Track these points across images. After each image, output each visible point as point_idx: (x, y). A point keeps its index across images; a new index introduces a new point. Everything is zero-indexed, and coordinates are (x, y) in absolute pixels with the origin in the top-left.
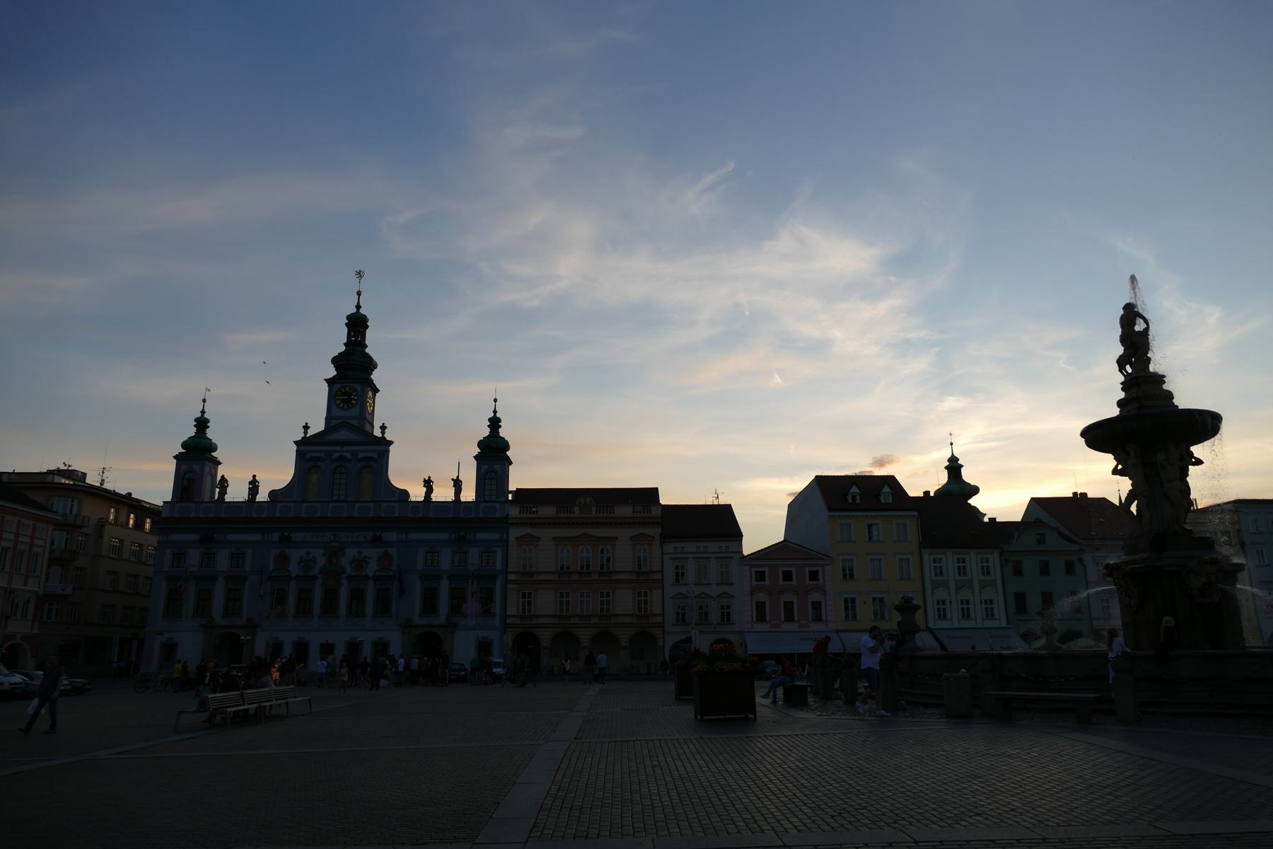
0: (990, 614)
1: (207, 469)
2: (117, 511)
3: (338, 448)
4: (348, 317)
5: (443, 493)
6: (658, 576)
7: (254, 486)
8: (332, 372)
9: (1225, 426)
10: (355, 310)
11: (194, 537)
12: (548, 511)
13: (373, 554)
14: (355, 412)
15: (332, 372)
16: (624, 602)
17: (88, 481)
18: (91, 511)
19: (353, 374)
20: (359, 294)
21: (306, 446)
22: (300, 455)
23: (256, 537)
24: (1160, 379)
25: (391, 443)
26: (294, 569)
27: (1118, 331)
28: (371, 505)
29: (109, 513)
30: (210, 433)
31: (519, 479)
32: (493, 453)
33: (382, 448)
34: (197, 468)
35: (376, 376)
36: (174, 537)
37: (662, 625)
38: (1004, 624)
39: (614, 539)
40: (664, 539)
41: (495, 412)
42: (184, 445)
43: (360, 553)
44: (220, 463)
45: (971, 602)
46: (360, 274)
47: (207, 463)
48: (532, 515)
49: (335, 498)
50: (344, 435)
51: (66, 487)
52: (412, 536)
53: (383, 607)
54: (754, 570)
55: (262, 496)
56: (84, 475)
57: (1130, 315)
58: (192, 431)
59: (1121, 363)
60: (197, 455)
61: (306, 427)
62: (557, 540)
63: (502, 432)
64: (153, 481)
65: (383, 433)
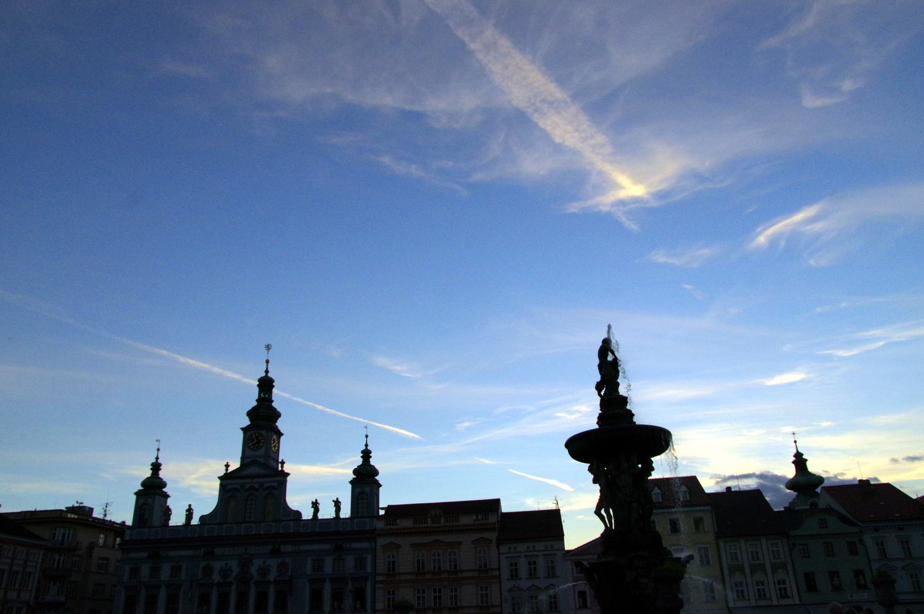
0: (784, 594)
2: (106, 536)
4: (260, 380)
5: (327, 512)
6: (496, 573)
7: (190, 513)
8: (246, 422)
9: (678, 436)
10: (264, 374)
11: (145, 555)
12: (407, 523)
13: (273, 563)
14: (262, 452)
15: (246, 422)
16: (469, 595)
17: (95, 515)
18: (84, 537)
19: (263, 424)
20: (267, 362)
21: (227, 479)
22: (222, 487)
24: (624, 400)
25: (288, 474)
26: (216, 577)
27: (597, 361)
29: (98, 538)
30: (162, 474)
31: (387, 498)
32: (365, 479)
34: (150, 501)
35: (280, 424)
36: (133, 555)
38: (797, 601)
39: (460, 543)
40: (499, 542)
41: (366, 445)
42: (143, 484)
44: (169, 496)
45: (766, 582)
46: (268, 347)
47: (157, 497)
48: (394, 527)
49: (247, 519)
50: (254, 470)
51: (80, 517)
55: (195, 521)
56: (91, 510)
57: (606, 348)
59: (599, 387)
60: (153, 491)
61: (227, 466)
62: (413, 545)
63: (373, 462)
64: (123, 513)
65: (282, 467)
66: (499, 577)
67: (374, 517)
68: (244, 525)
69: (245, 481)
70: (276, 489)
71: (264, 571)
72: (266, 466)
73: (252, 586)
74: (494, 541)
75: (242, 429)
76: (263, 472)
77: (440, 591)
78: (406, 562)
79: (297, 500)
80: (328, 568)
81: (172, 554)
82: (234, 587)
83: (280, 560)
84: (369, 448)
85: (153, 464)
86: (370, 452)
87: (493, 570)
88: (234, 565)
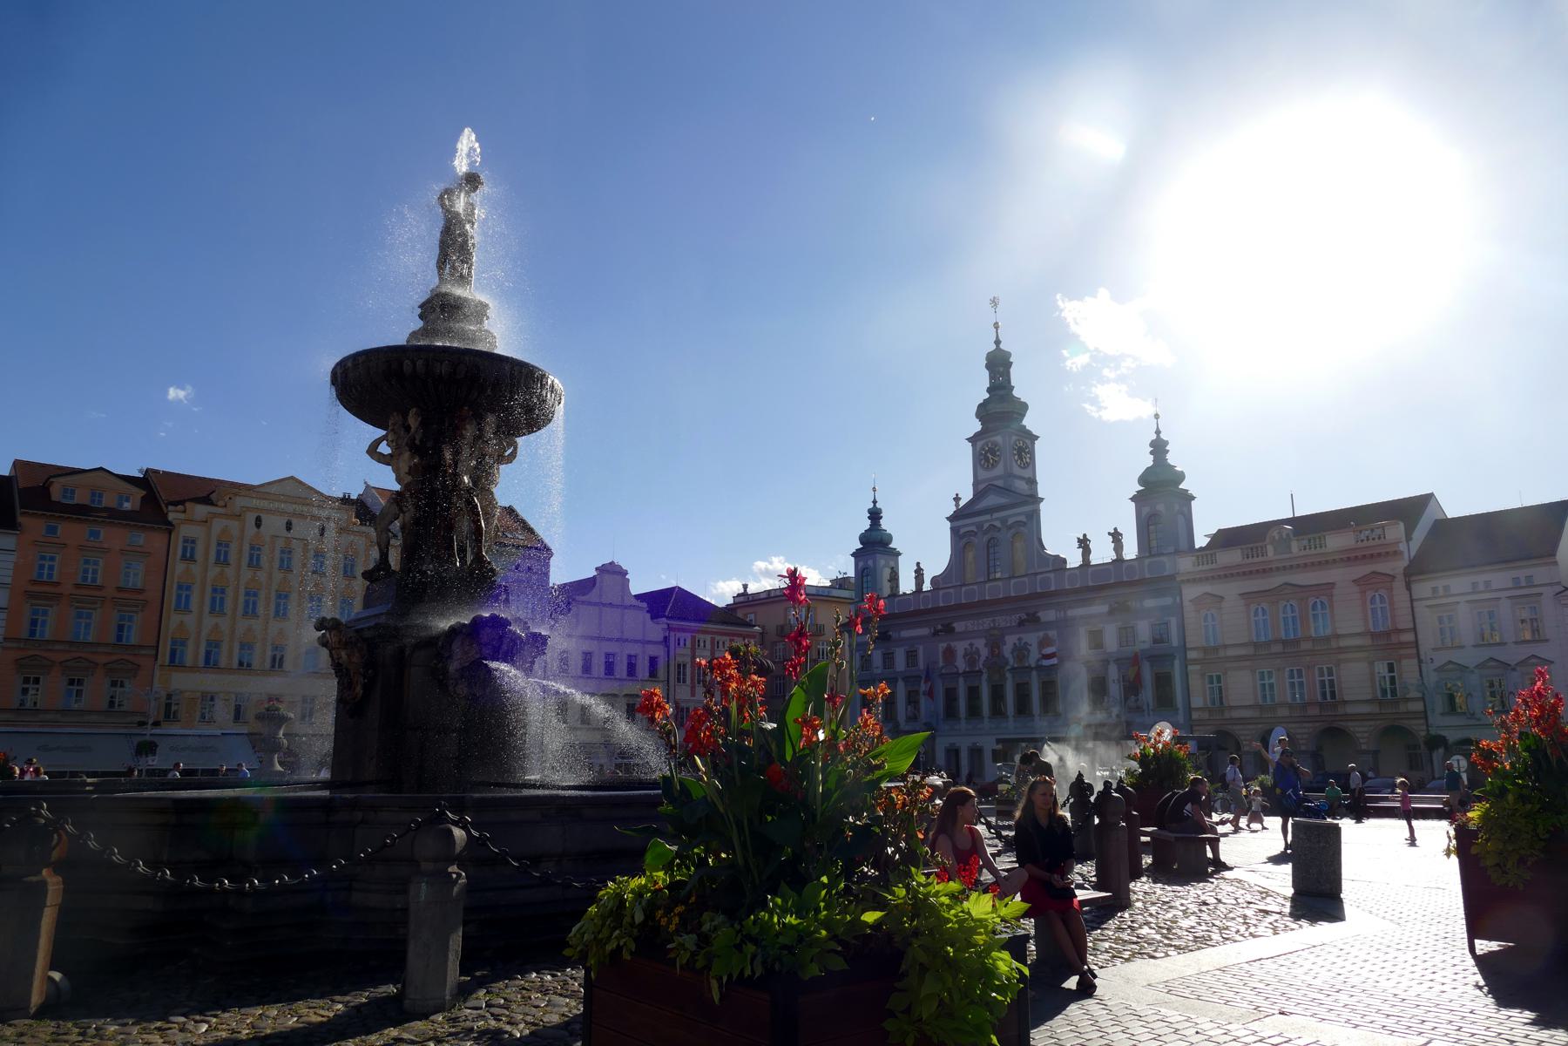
1: (882, 562)
3: (988, 517)
5: (1102, 553)
6: (1409, 637)
7: (919, 573)
12: (1233, 557)
13: (1032, 638)
14: (999, 470)
20: (996, 326)
23: (924, 631)
26: (961, 665)
34: (870, 563)
35: (1029, 422)
37: (1424, 715)
41: (1158, 432)
55: (927, 586)
58: (867, 524)
61: (957, 499)
63: (1171, 459)
66: (1416, 644)
67: (1177, 552)
69: (977, 519)
72: (1006, 490)
73: (1008, 675)
75: (969, 440)
76: (1002, 501)
77: (1300, 676)
79: (1059, 538)
81: (905, 634)
82: (985, 676)
84: (1163, 436)
85: (870, 511)
86: (1167, 443)
88: (980, 644)
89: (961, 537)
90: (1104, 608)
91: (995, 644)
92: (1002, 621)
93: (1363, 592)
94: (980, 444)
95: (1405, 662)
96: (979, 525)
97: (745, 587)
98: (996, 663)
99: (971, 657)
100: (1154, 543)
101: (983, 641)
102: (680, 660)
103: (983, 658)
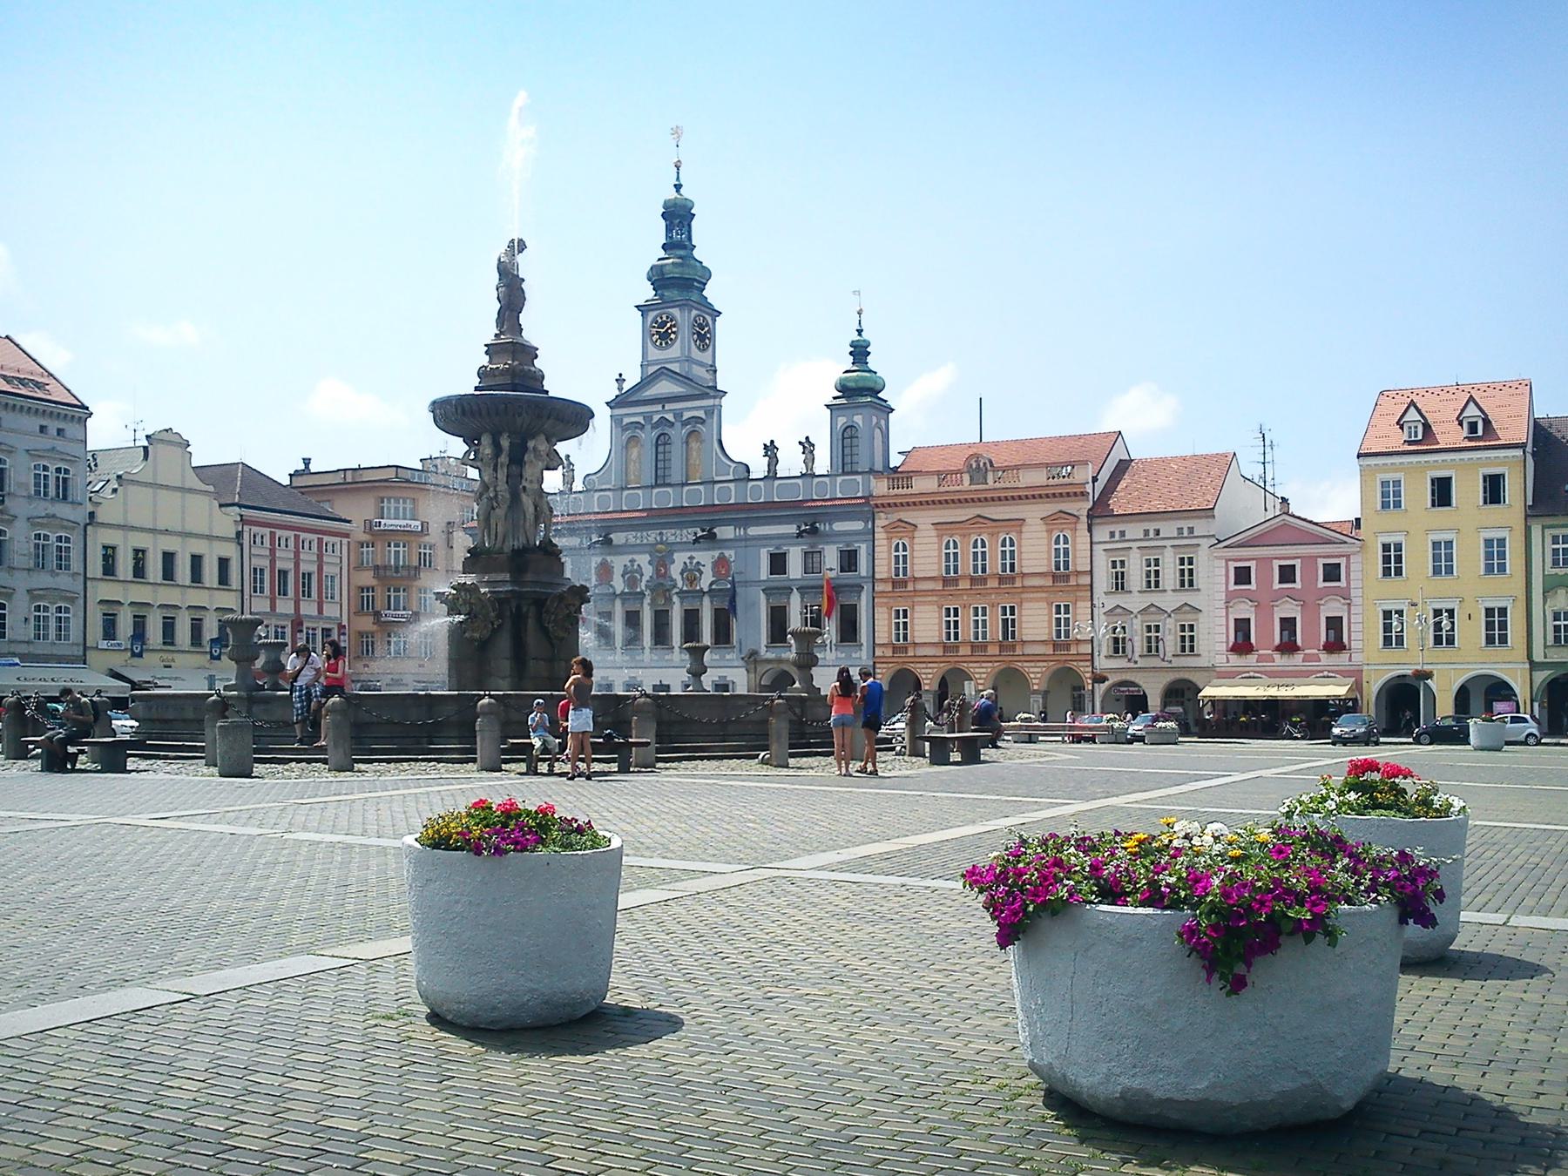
3: (659, 407)
5: (791, 462)
13: (706, 558)
14: (675, 351)
26: (619, 585)
28: (701, 487)
32: (860, 395)
33: (710, 402)
43: (691, 558)
52: (753, 531)
53: (722, 635)
54: (1232, 565)
61: (620, 380)
67: (872, 471)
68: (656, 491)
70: (703, 422)
71: (691, 573)
72: (684, 378)
73: (675, 599)
74: (1084, 519)
77: (984, 614)
78: (927, 558)
79: (741, 440)
80: (795, 568)
82: (647, 600)
83: (716, 554)
87: (1078, 573)
88: (643, 560)
89: (625, 428)
90: (792, 529)
91: (662, 562)
92: (671, 535)
93: (1050, 532)
94: (652, 315)
95: (1079, 604)
96: (648, 417)
97: (307, 462)
98: (661, 587)
99: (631, 576)
100: (848, 459)
101: (648, 557)
102: (257, 562)
103: (646, 578)
